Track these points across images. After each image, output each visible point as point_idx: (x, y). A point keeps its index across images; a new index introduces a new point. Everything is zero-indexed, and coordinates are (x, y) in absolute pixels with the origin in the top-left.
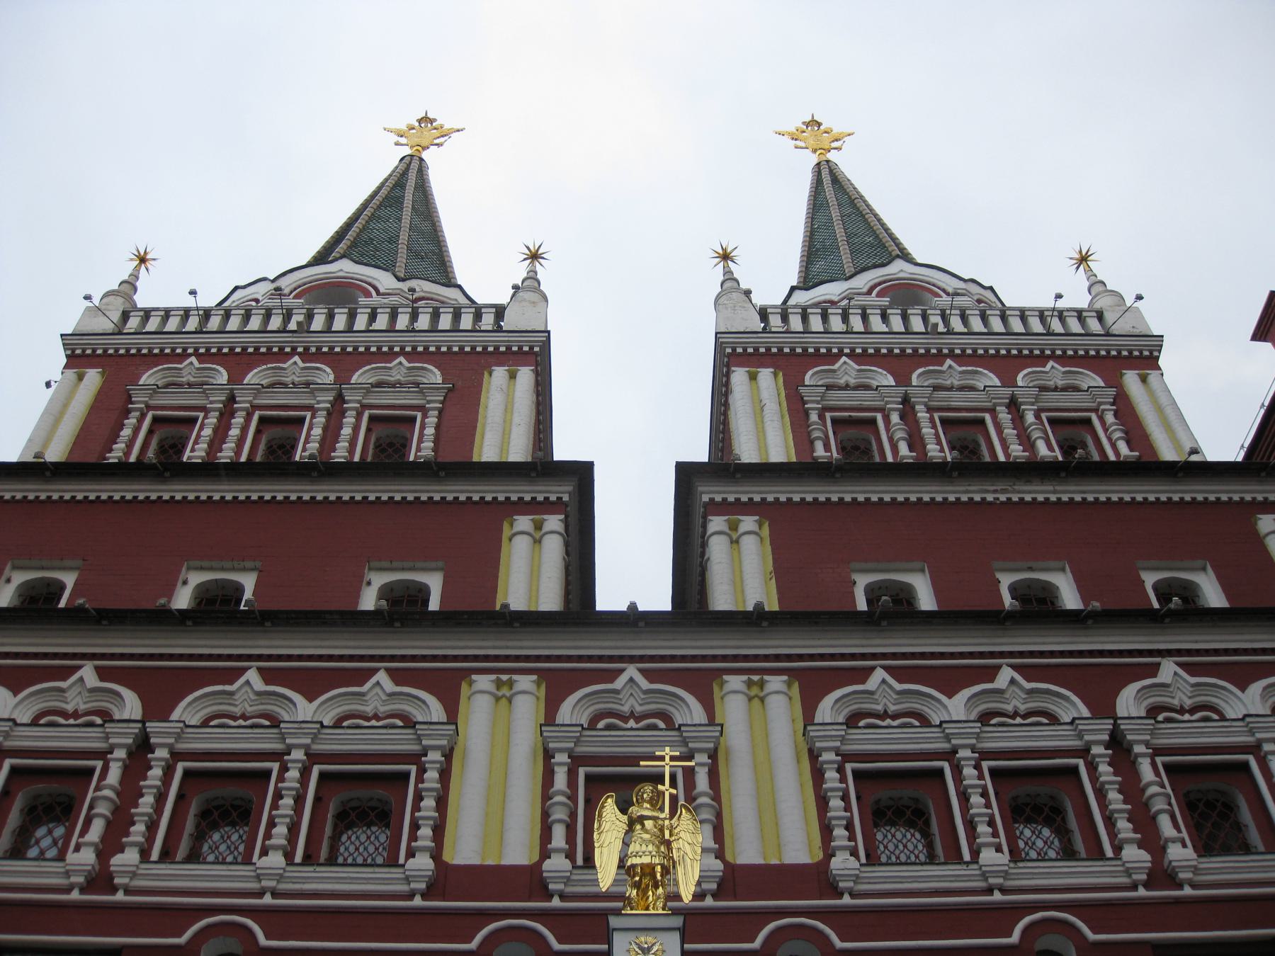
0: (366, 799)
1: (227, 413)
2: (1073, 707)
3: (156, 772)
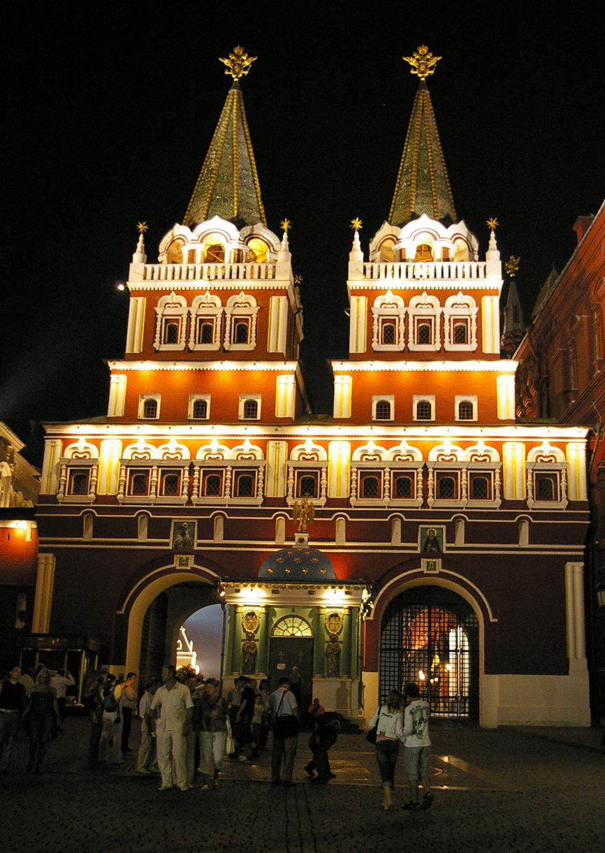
3: (196, 473)
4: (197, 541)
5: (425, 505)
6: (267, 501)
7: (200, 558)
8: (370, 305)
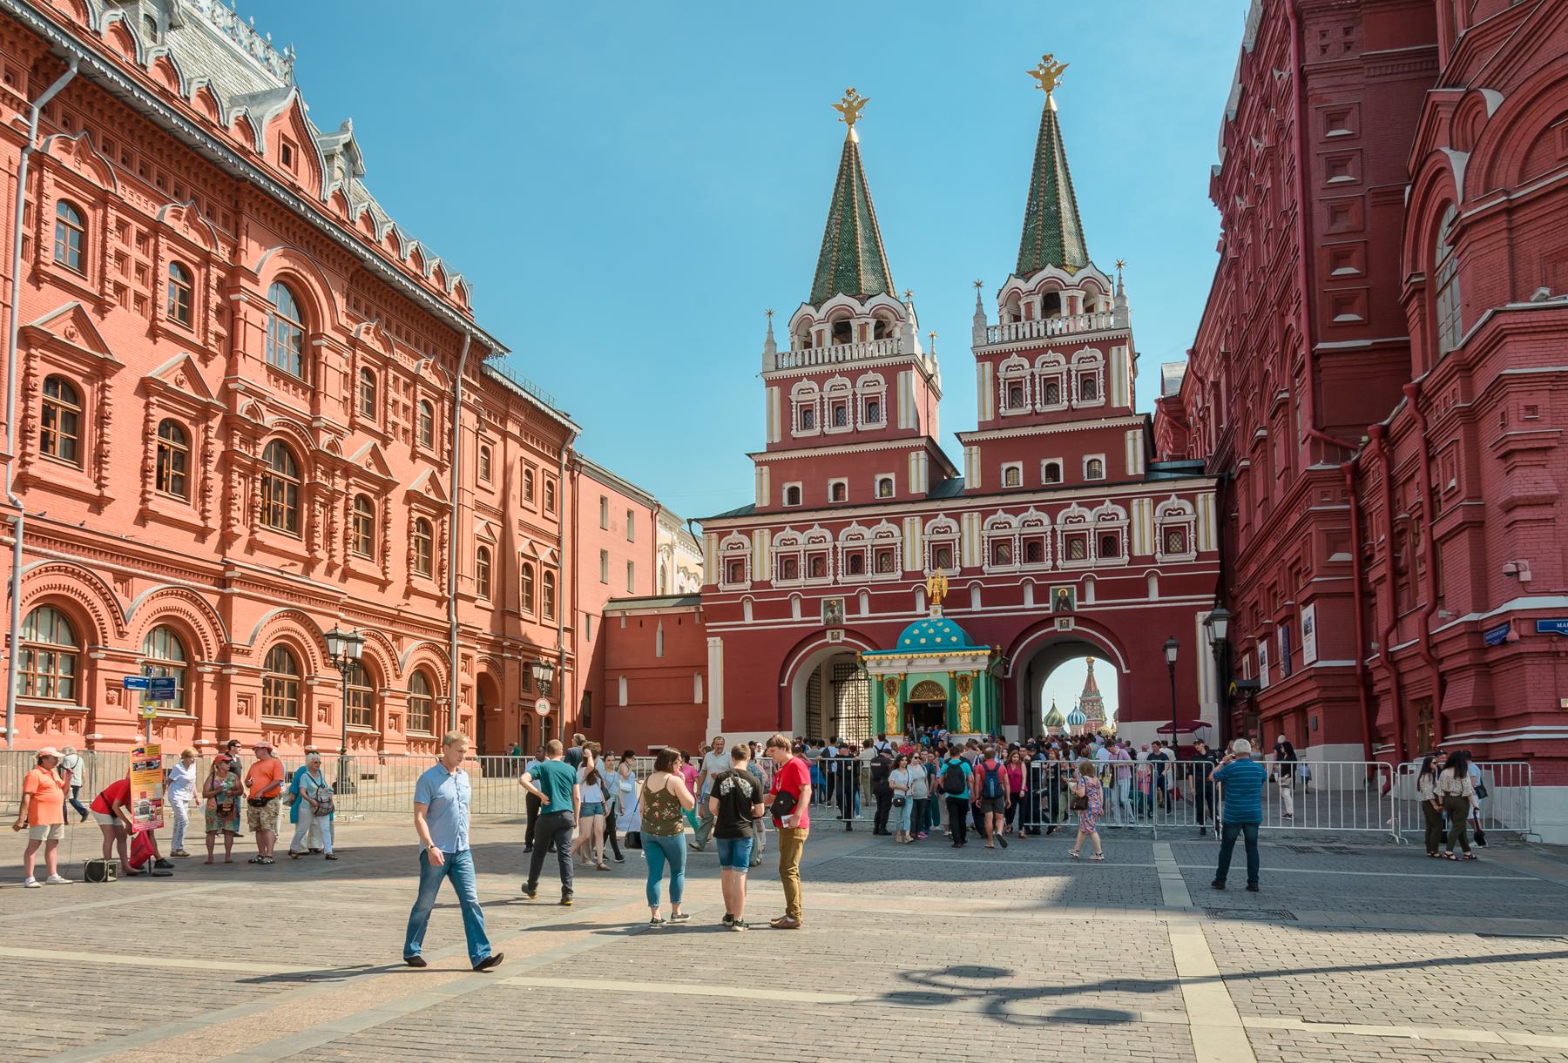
0: (885, 556)
1: (822, 404)
2: (1046, 519)
4: (845, 616)
5: (1055, 567)
6: (905, 575)
7: (850, 632)
8: (996, 369)
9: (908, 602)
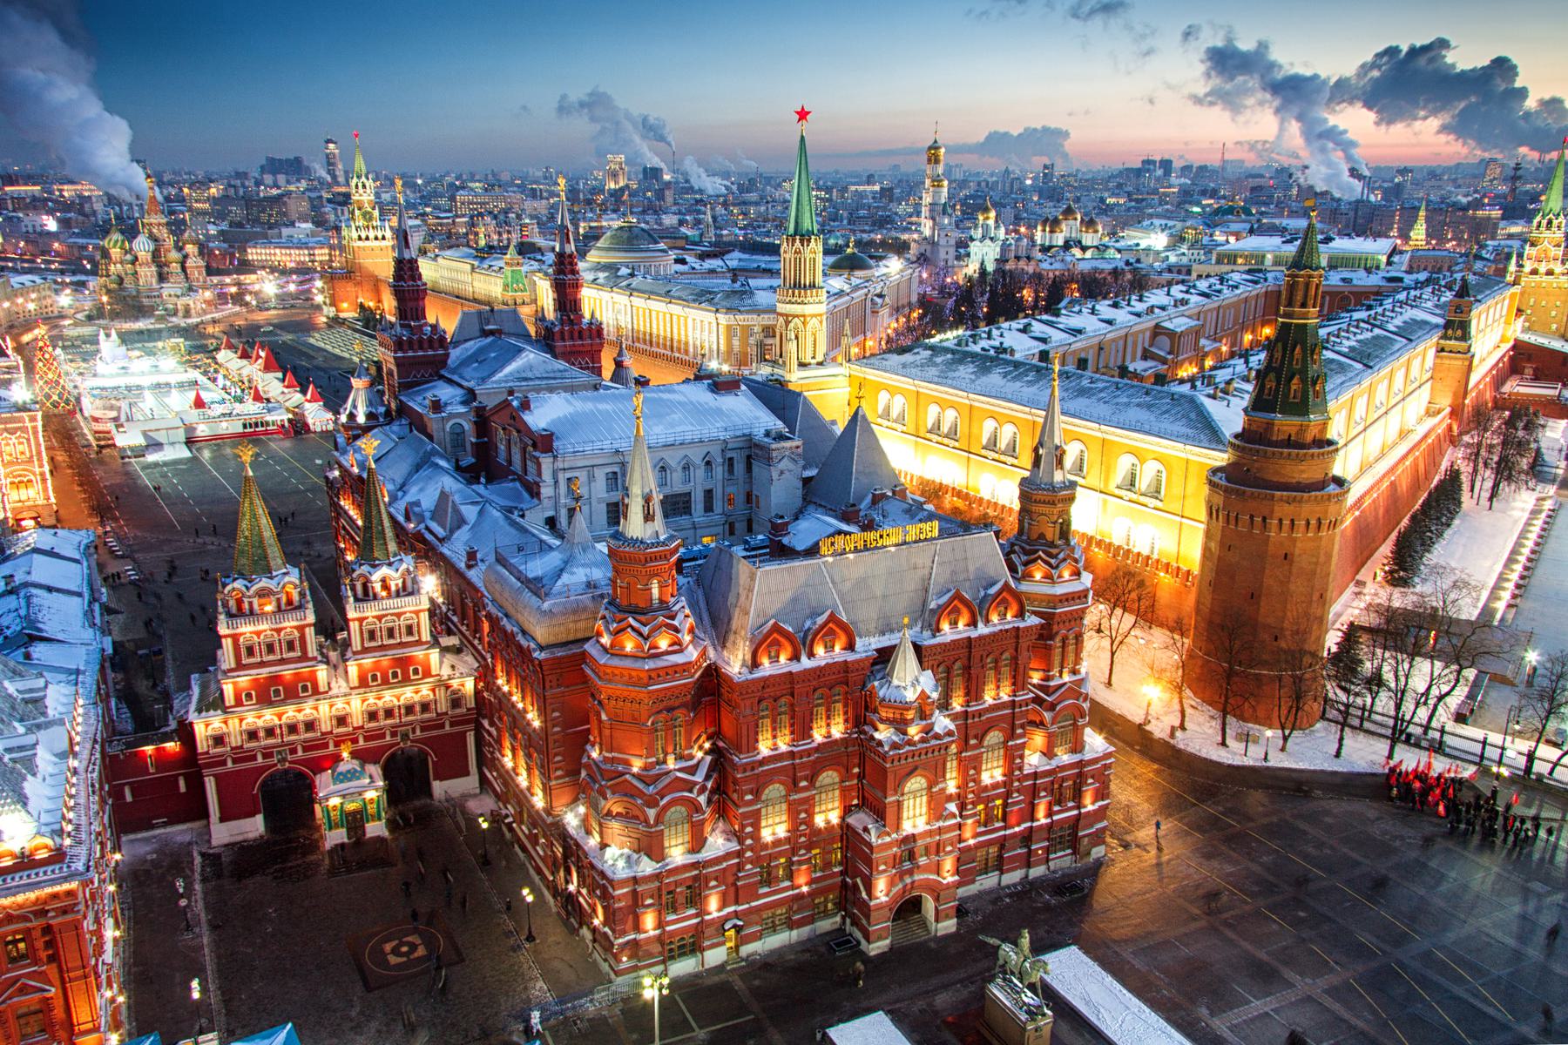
9: (326, 746)
